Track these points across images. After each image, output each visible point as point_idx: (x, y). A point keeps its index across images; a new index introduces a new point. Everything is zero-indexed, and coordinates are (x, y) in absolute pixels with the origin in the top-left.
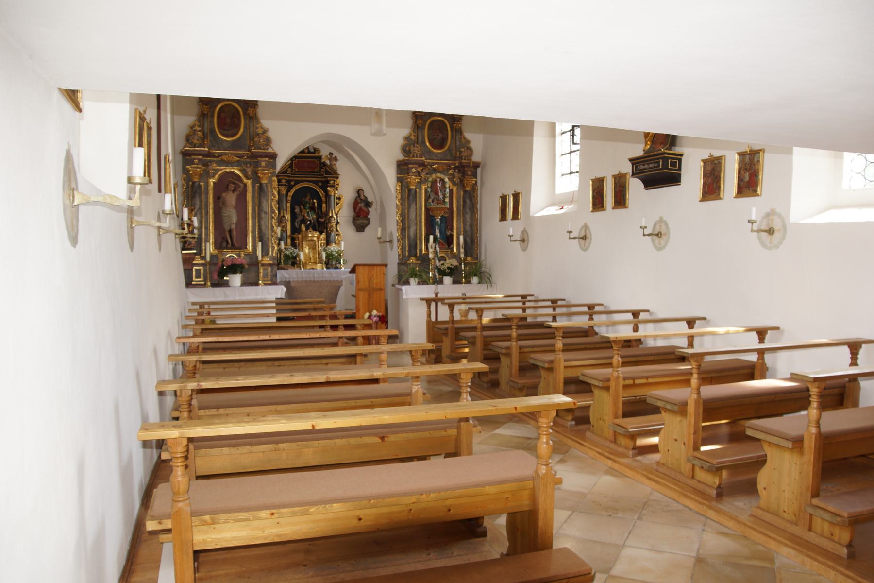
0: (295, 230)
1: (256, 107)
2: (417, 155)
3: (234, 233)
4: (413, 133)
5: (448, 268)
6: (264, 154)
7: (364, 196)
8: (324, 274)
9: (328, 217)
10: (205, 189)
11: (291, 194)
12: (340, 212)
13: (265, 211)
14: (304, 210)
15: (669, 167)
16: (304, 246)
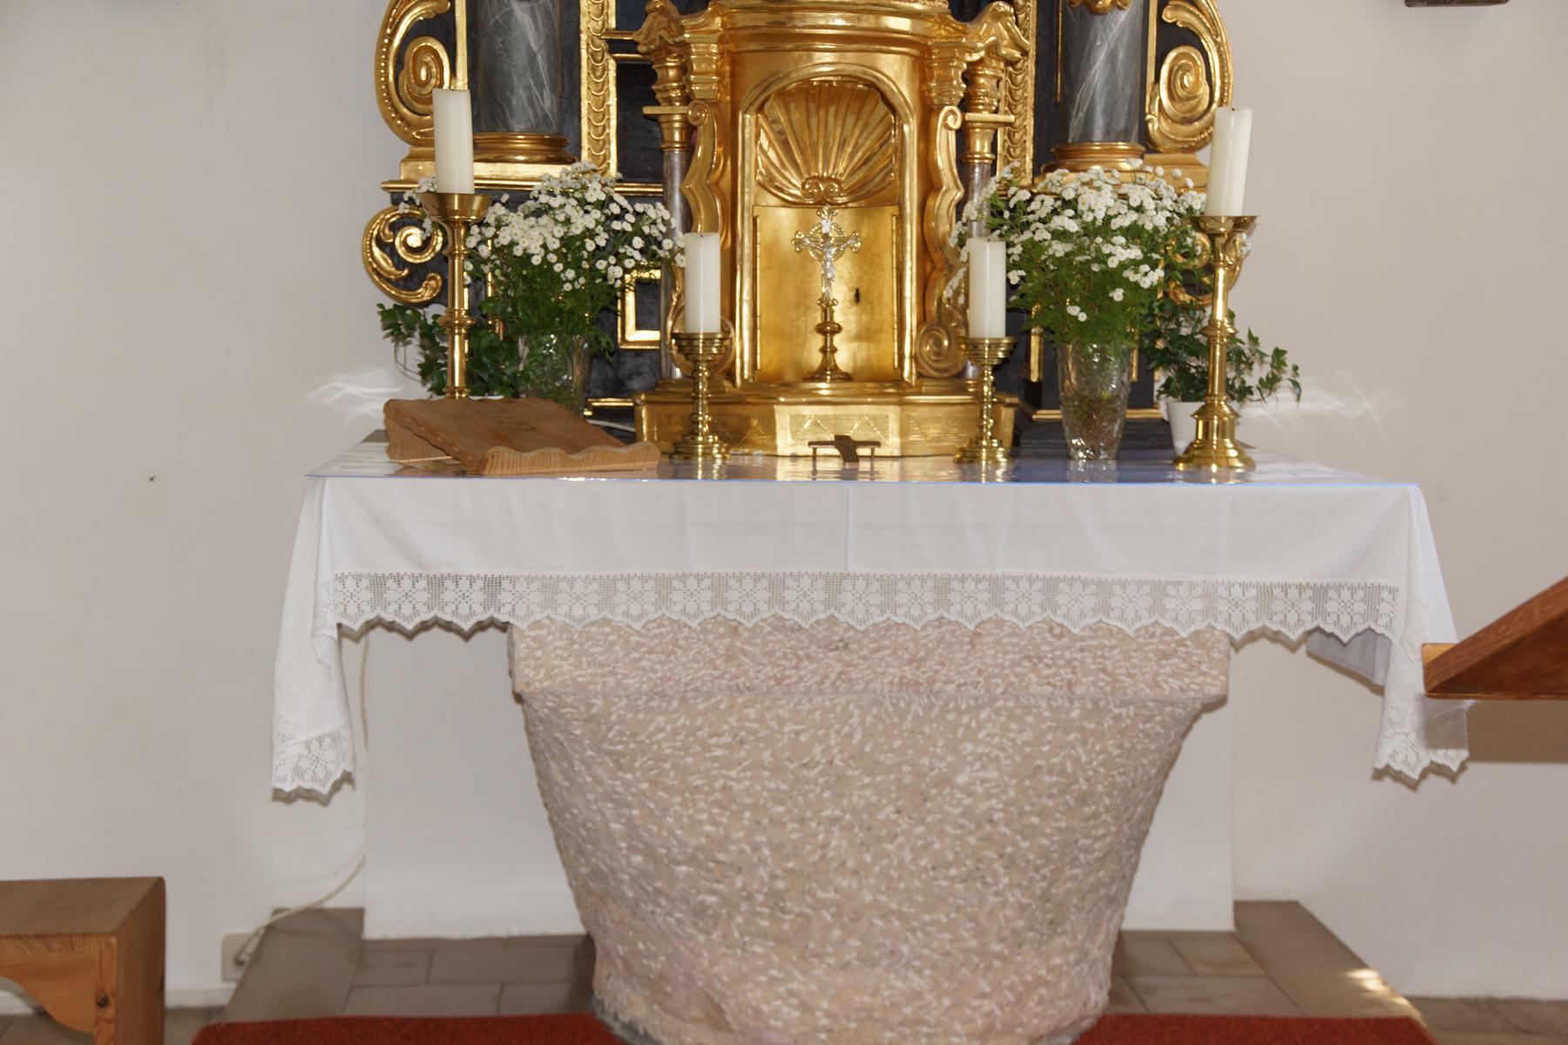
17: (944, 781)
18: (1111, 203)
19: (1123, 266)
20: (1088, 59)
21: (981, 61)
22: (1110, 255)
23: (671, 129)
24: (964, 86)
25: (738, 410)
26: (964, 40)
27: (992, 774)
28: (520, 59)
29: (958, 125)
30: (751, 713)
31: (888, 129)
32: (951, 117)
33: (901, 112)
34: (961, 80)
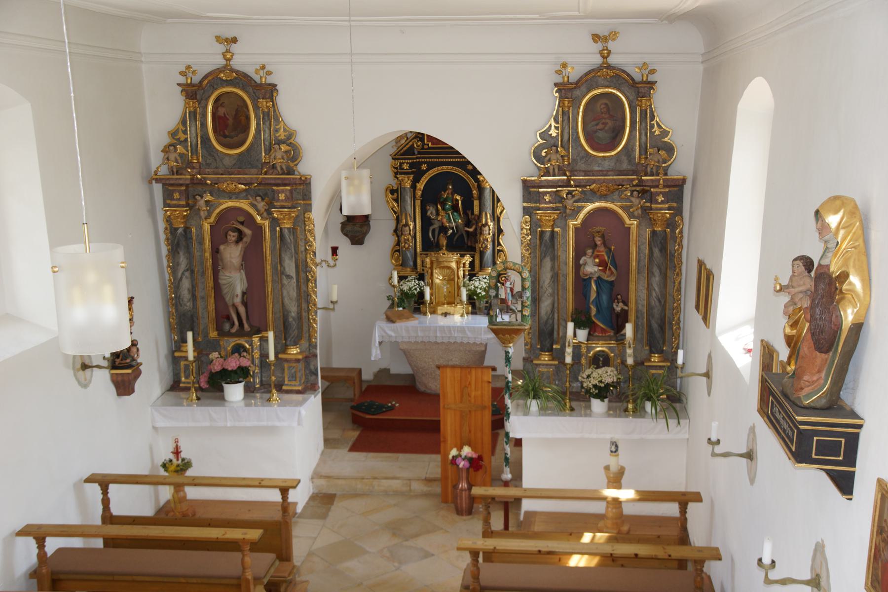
0: (430, 246)
1: (275, 94)
2: (554, 169)
3: (242, 310)
4: (553, 124)
5: (595, 386)
6: (279, 182)
8: (452, 332)
9: (480, 225)
10: (197, 236)
11: (421, 186)
13: (288, 274)
14: (442, 213)
15: (814, 456)
16: (436, 275)
17: (452, 360)
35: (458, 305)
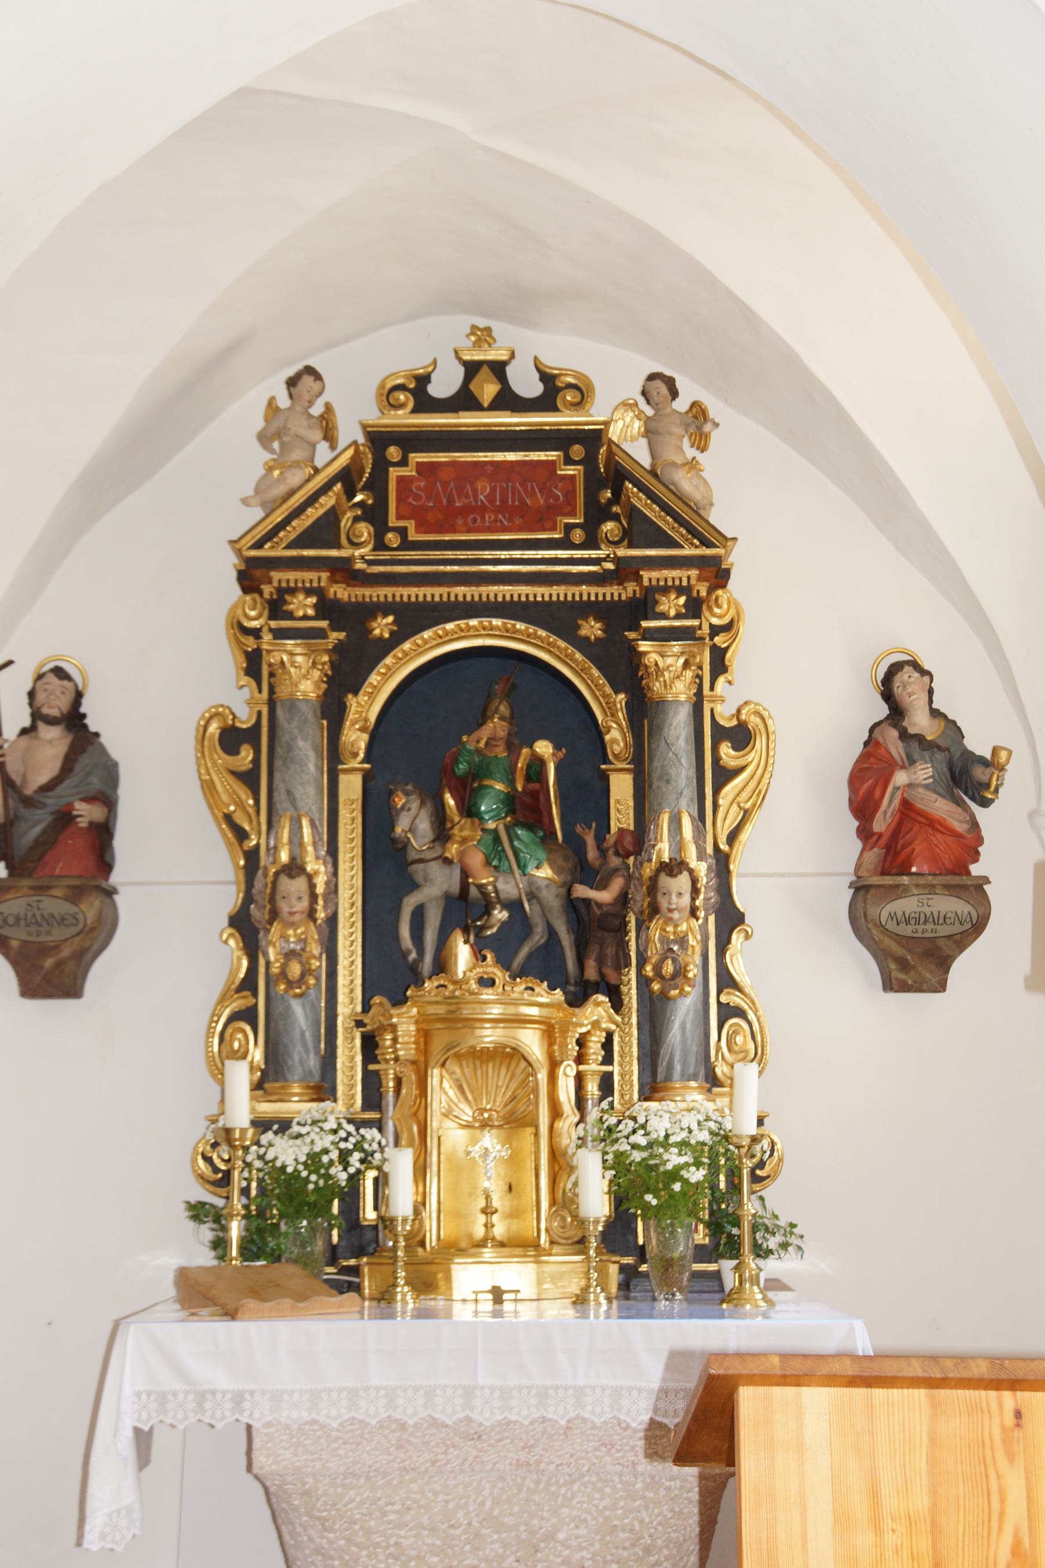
7: (935, 713)
12: (744, 836)
17: (550, 1537)
18: (668, 1126)
19: (679, 1168)
20: (667, 1028)
21: (588, 1032)
22: (668, 1160)
23: (387, 1079)
24: (577, 1048)
25: (427, 1268)
26: (574, 1020)
27: (583, 1532)
28: (297, 1035)
29: (574, 1073)
30: (415, 1487)
31: (528, 1077)
32: (569, 1069)
33: (535, 1066)
34: (574, 1044)
35: (556, 1249)
